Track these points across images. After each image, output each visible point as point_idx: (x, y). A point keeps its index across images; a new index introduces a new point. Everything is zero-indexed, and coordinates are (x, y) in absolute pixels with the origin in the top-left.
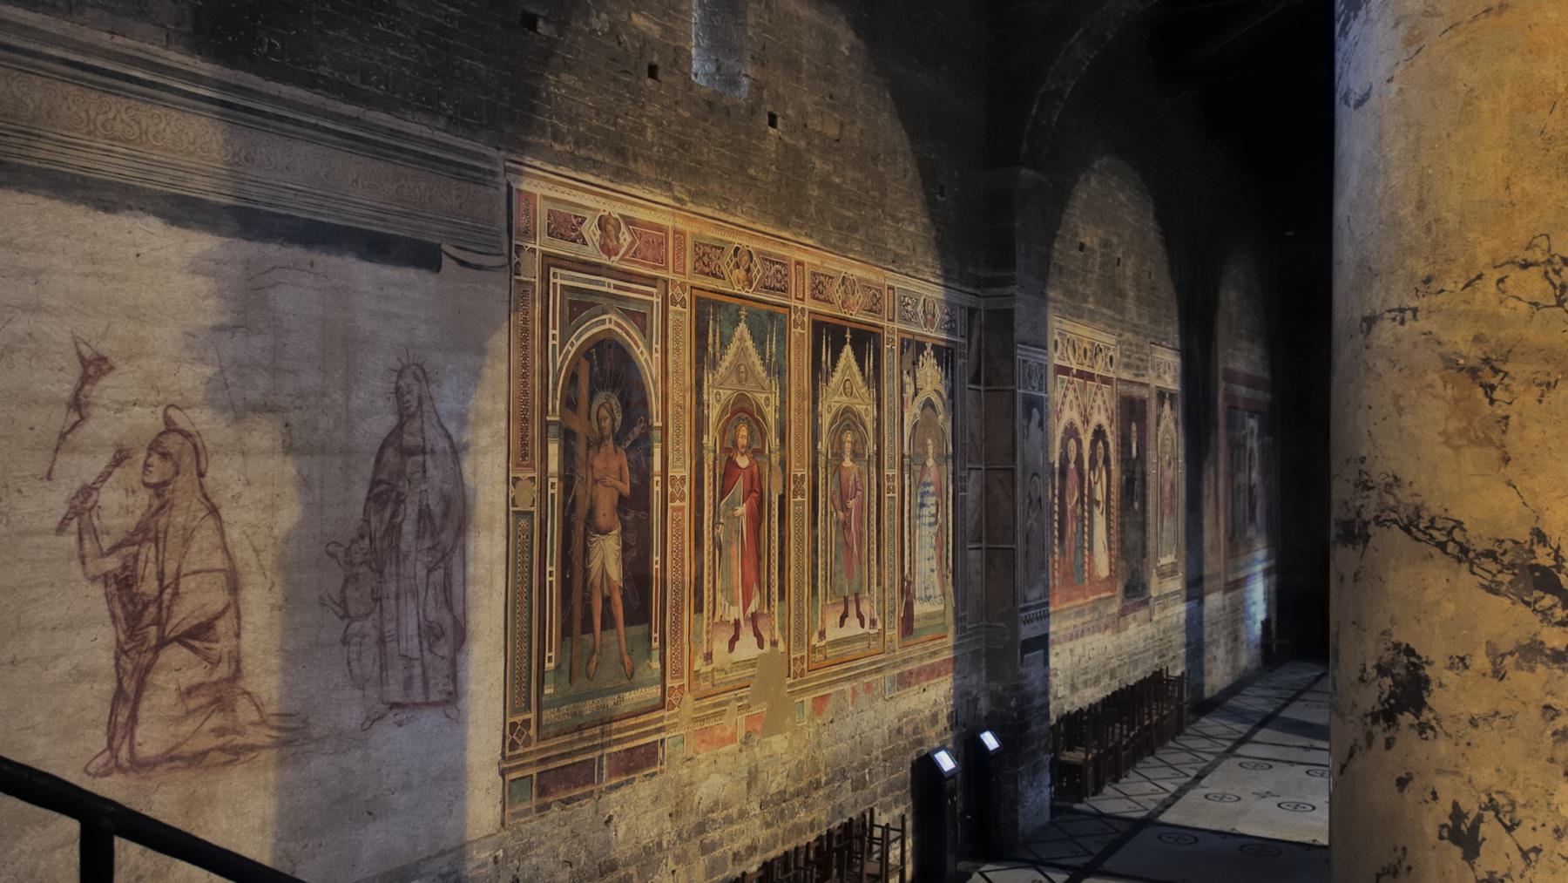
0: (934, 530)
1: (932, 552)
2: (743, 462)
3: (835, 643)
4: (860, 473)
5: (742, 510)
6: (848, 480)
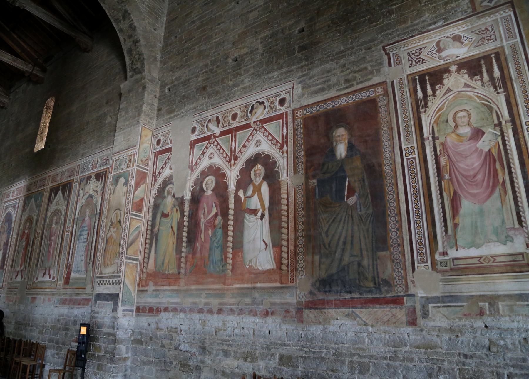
0: (86, 244)
1: (83, 253)
2: (26, 231)
4: (57, 228)
5: (24, 243)
6: (53, 231)
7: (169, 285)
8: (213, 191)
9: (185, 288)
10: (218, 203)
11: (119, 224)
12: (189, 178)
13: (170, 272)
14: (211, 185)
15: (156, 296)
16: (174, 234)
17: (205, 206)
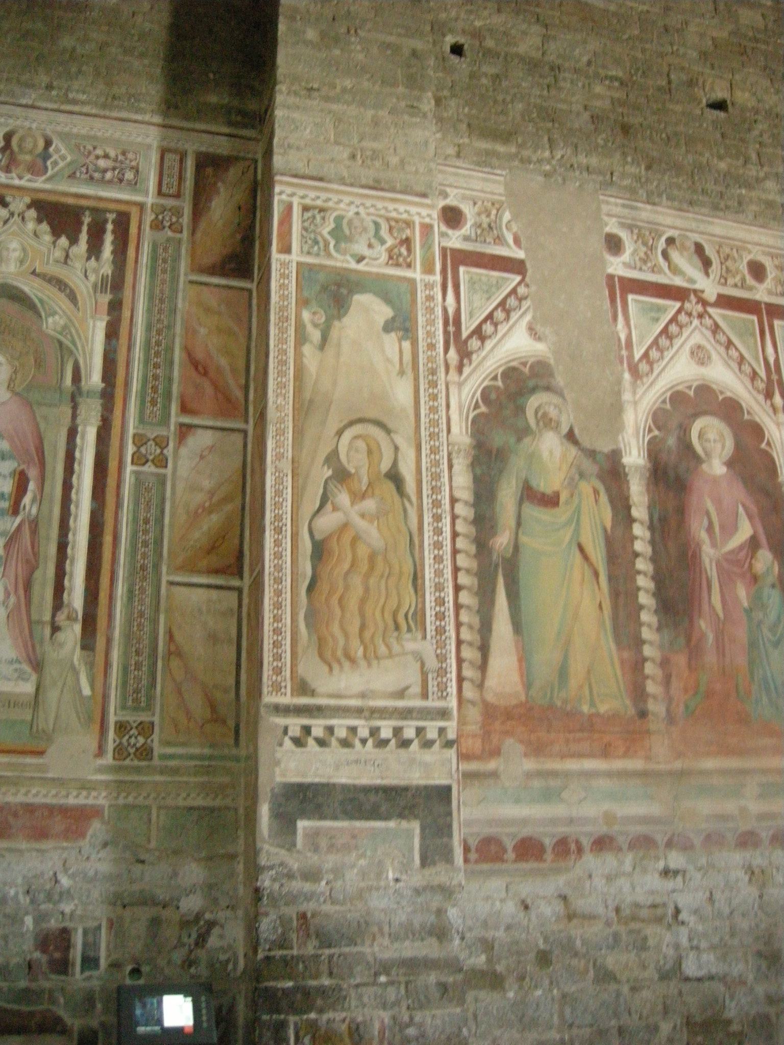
7: (606, 752)
8: (730, 464)
9: (678, 765)
10: (754, 509)
11: (390, 486)
12: (627, 396)
13: (603, 708)
14: (719, 446)
15: (548, 796)
16: (596, 574)
17: (710, 506)
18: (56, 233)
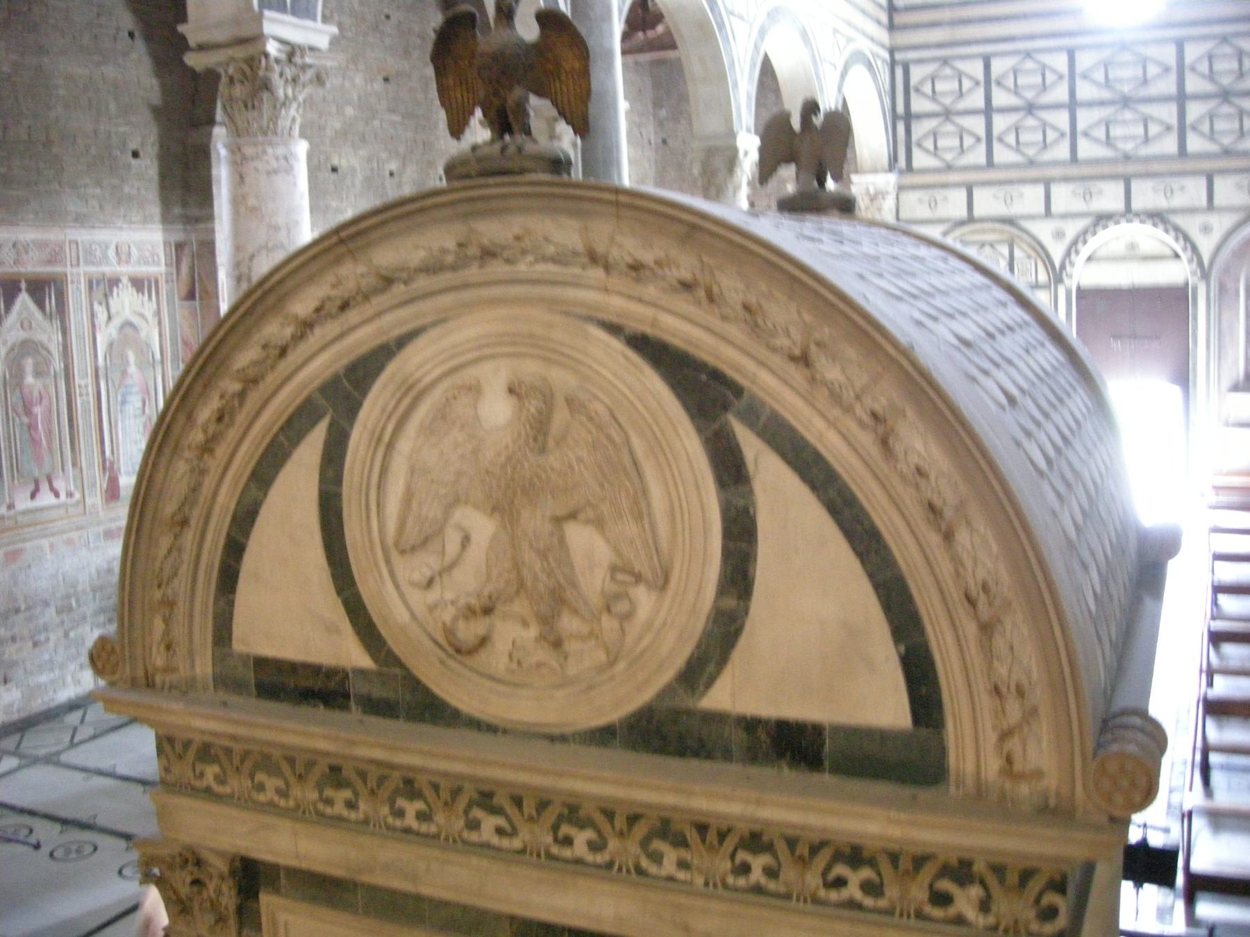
3: (24, 513)
4: (45, 387)
6: (31, 393)
18: (138, 292)
